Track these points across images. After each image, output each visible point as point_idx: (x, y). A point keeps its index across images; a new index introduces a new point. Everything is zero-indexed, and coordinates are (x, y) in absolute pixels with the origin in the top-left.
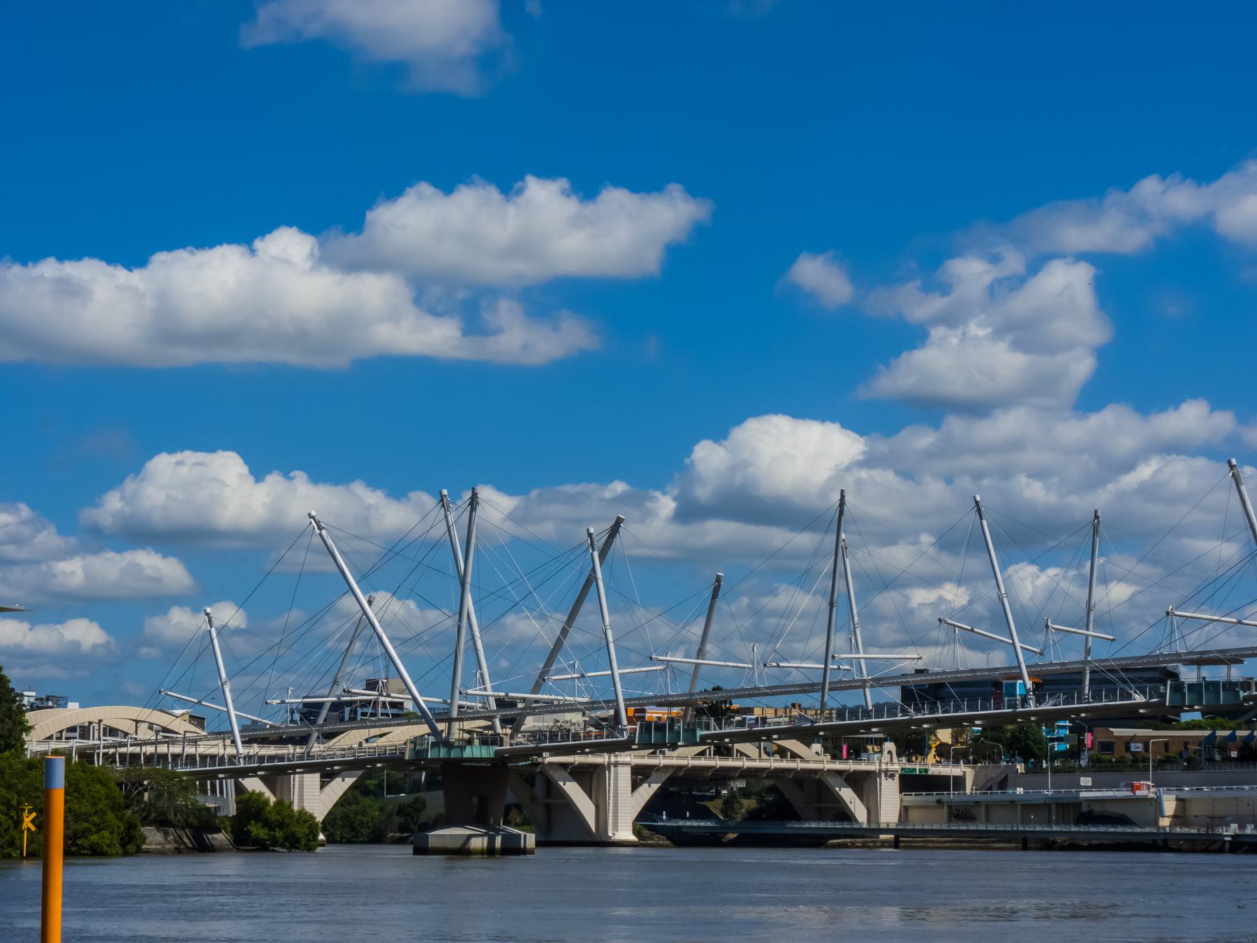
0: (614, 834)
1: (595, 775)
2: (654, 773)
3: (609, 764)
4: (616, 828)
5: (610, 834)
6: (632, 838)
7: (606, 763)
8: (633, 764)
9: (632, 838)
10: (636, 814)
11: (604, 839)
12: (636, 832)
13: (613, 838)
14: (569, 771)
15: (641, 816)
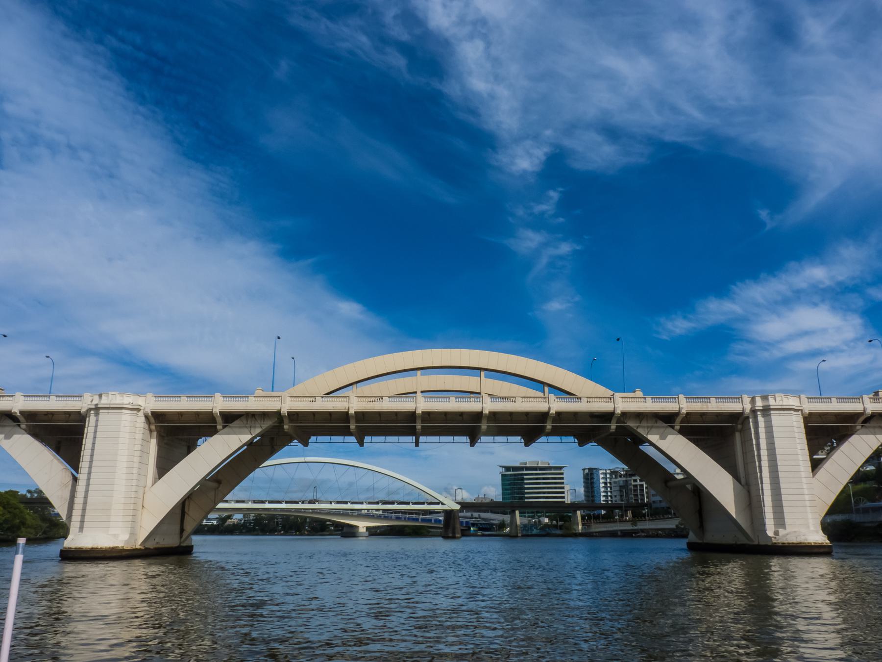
0: (776, 533)
1: (737, 435)
2: (859, 427)
3: (754, 411)
4: (780, 521)
5: (770, 533)
6: (818, 537)
7: (747, 411)
8: (806, 411)
9: (818, 537)
10: (831, 499)
11: (762, 543)
12: (826, 527)
13: (774, 541)
14: (678, 427)
15: (840, 505)
